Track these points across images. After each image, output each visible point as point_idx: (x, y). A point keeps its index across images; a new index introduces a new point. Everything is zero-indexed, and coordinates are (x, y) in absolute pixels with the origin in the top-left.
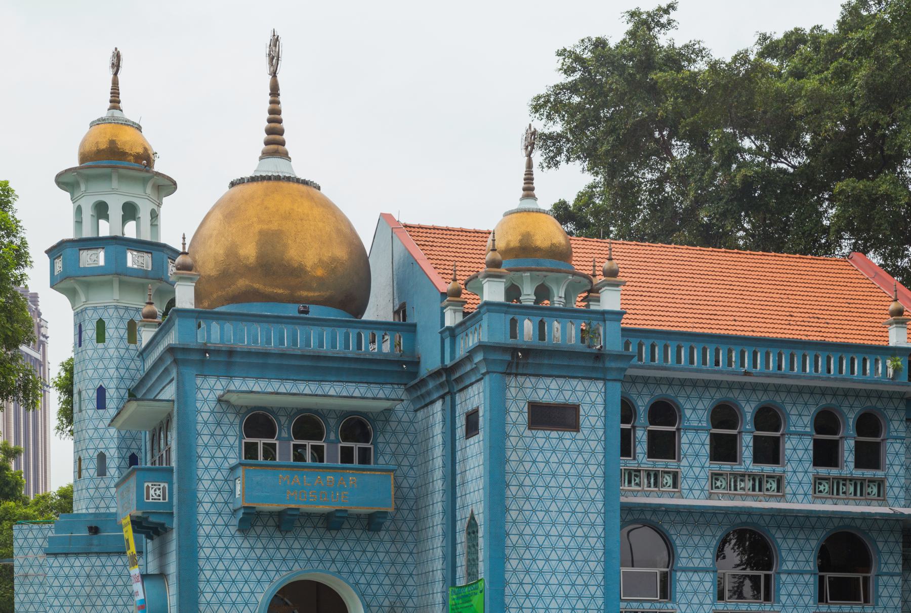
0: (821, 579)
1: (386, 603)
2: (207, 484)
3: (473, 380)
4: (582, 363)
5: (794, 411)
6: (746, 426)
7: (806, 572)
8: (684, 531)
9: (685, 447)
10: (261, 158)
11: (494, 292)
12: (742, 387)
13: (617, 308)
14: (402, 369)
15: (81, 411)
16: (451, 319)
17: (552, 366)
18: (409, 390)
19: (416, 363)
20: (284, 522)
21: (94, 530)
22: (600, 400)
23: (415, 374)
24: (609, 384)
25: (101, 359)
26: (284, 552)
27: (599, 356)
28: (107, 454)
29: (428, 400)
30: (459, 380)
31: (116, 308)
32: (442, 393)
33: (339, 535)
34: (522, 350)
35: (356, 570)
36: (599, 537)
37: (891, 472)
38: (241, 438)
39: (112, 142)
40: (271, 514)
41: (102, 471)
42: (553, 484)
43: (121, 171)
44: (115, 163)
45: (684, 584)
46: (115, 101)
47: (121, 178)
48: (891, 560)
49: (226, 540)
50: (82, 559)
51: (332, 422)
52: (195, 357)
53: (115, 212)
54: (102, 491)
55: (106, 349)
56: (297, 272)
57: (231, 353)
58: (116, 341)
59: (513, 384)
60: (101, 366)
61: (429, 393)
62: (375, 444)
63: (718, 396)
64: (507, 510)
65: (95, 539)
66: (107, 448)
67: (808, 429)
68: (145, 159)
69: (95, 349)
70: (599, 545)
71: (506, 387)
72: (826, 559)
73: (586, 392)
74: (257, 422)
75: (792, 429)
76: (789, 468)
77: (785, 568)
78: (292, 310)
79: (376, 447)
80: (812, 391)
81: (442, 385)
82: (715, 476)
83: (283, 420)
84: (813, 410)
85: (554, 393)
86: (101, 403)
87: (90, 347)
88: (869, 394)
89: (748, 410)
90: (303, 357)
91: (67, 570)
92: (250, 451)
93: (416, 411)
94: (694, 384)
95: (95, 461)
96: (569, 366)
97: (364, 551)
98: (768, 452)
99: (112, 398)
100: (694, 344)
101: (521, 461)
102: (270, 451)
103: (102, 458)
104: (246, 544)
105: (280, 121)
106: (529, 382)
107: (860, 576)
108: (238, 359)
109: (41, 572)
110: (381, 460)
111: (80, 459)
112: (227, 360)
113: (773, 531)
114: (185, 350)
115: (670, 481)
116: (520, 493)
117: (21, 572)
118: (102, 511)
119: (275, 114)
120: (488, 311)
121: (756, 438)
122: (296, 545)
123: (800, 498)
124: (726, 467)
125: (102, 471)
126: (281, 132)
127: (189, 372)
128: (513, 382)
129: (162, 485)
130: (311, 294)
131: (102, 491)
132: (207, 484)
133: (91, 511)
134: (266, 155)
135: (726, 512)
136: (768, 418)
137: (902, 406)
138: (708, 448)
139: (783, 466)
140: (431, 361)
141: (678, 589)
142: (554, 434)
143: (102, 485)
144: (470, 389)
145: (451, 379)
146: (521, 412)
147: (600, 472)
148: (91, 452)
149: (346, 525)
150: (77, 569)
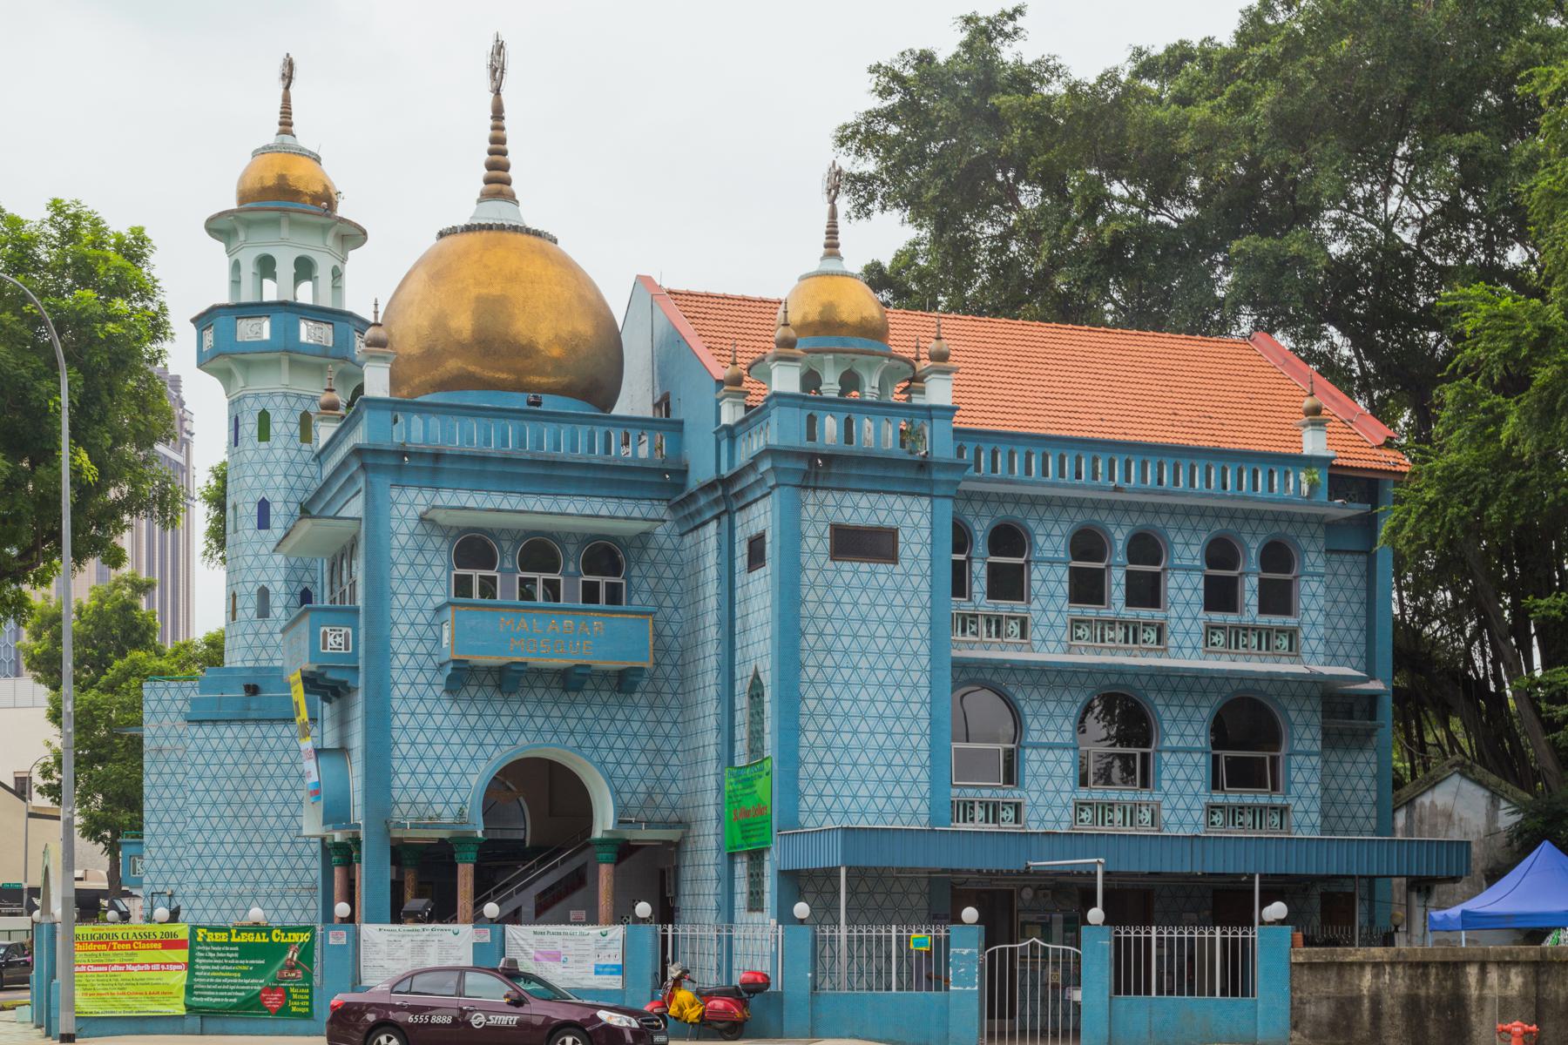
0: (1216, 759)
1: (642, 788)
2: (404, 629)
3: (758, 494)
4: (901, 474)
5: (1179, 539)
6: (1116, 559)
7: (1196, 750)
8: (1035, 695)
9: (1036, 585)
10: (479, 201)
11: (786, 379)
12: (1111, 506)
13: (948, 402)
14: (666, 482)
15: (236, 531)
16: (730, 414)
17: (862, 478)
18: (673, 508)
19: (683, 472)
20: (507, 681)
21: (252, 690)
22: (925, 522)
23: (682, 487)
24: (937, 502)
25: (265, 463)
26: (506, 720)
27: (924, 465)
28: (271, 589)
29: (698, 521)
31: (285, 395)
32: (716, 511)
33: (580, 698)
34: (823, 457)
35: (603, 744)
36: (923, 703)
37: (1307, 619)
38: (450, 569)
39: (282, 177)
40: (489, 670)
41: (264, 611)
42: (863, 632)
43: (293, 215)
44: (285, 204)
45: (1035, 765)
46: (286, 124)
47: (293, 224)
48: (1307, 735)
49: (429, 704)
50: (236, 728)
51: (571, 549)
52: (392, 461)
53: (285, 268)
54: (263, 637)
55: (271, 449)
56: (526, 350)
57: (437, 456)
58: (284, 440)
59: (811, 500)
60: (264, 471)
61: (699, 512)
62: (628, 578)
63: (1080, 518)
64: (802, 666)
65: (254, 702)
66: (270, 581)
67: (1198, 563)
68: (325, 200)
69: (256, 450)
70: (924, 713)
71: (801, 504)
72: (1221, 734)
73: (907, 511)
74: (473, 548)
75: (1177, 562)
76: (1172, 613)
77: (1167, 744)
78: (519, 401)
79: (629, 583)
80: (1202, 512)
81: (716, 502)
82: (1076, 623)
83: (506, 545)
84: (1204, 537)
85: (864, 513)
86: (263, 522)
87: (249, 446)
88: (1277, 517)
89: (1120, 538)
90: (533, 463)
91: (215, 742)
92: (463, 586)
93: (682, 535)
94: (1048, 502)
95: (255, 598)
96: (884, 478)
97: (613, 720)
98: (1145, 591)
99: (277, 514)
100: (1048, 451)
101: (821, 602)
102: (488, 587)
103: (264, 593)
104: (456, 710)
105: (504, 153)
106: (831, 499)
107: (1267, 755)
108: (446, 465)
109: (180, 746)
110: (636, 600)
111: (234, 595)
112: (432, 466)
113: (1152, 696)
114: (377, 452)
115: (1017, 630)
116: (820, 645)
117: (153, 746)
118: (264, 664)
119: (498, 144)
120: (780, 404)
121: (1129, 574)
122: (522, 711)
123: (1187, 652)
124: (1091, 611)
125: (264, 611)
126: (506, 168)
127: (382, 481)
128: (810, 497)
129: (344, 630)
130: (544, 380)
131: (263, 637)
132: (404, 629)
133: (248, 664)
134: (486, 196)
135: (1091, 671)
136: (1145, 547)
137: (1320, 532)
138: (1066, 586)
139: (1165, 610)
140: (702, 470)
141: (1028, 771)
142: (865, 567)
143: (264, 630)
145: (728, 493)
146: (821, 538)
147: (924, 617)
148: (249, 586)
149: (588, 685)
150: (229, 742)
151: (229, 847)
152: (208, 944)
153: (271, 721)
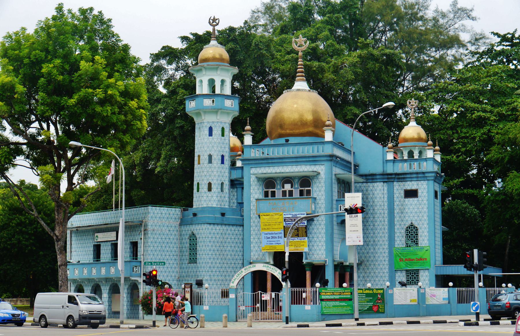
50: (220, 226)
61: (376, 179)
65: (224, 218)
69: (221, 139)
81: (388, 178)
117: (152, 228)
118: (223, 206)
133: (219, 206)
143: (223, 196)
144: (409, 182)
148: (219, 181)
151: (218, 264)
153: (229, 225)
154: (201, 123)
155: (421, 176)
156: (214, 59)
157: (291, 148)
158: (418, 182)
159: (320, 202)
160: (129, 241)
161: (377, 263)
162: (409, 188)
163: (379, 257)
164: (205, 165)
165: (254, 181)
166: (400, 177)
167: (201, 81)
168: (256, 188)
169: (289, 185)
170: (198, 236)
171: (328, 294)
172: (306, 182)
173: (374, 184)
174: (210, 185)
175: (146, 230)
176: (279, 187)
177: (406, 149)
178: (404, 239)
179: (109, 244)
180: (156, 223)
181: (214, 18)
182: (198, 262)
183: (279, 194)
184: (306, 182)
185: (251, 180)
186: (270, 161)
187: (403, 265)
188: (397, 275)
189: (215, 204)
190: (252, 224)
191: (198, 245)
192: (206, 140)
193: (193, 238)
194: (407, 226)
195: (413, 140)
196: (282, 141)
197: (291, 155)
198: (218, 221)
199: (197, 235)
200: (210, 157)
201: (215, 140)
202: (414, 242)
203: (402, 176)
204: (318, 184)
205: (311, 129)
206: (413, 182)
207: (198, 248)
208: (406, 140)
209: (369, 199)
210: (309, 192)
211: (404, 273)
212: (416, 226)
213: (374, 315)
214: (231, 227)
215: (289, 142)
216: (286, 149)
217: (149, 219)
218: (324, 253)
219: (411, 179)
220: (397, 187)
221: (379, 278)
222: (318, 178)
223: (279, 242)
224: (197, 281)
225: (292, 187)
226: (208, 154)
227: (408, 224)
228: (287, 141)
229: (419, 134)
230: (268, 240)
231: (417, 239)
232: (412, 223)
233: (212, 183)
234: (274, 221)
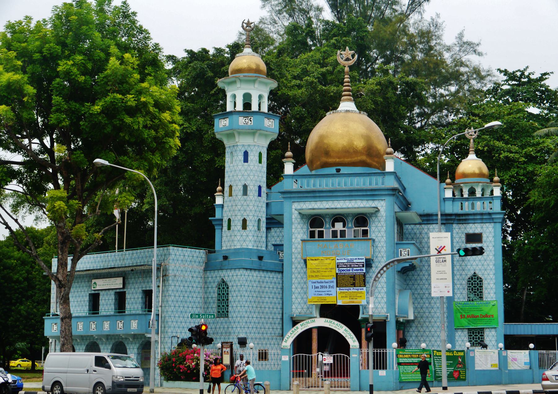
21: (260, 258)
30: (466, 220)
50: (257, 272)
109: (182, 275)
117: (173, 274)
118: (259, 248)
133: (255, 248)
143: (259, 235)
144: (471, 225)
148: (256, 217)
152: (437, 356)
154: (234, 146)
155: (486, 217)
156: (249, 70)
157: (343, 180)
158: (482, 224)
159: (380, 245)
160: (140, 289)
161: (433, 320)
162: (471, 232)
163: (435, 313)
164: (239, 197)
165: (296, 218)
166: (461, 218)
167: (234, 96)
168: (299, 227)
169: (341, 224)
170: (230, 284)
171: (406, 356)
172: (362, 220)
173: (429, 225)
174: (244, 221)
175: (165, 275)
176: (328, 226)
177: (466, 186)
178: (465, 292)
179: (112, 292)
180: (177, 267)
181: (248, 21)
182: (230, 315)
183: (328, 234)
184: (362, 220)
185: (293, 217)
186: (318, 195)
187: (464, 322)
188: (457, 334)
189: (250, 244)
190: (293, 270)
191: (230, 295)
192: (240, 167)
193: (223, 287)
194: (469, 276)
195: (473, 175)
196: (333, 170)
197: (344, 187)
198: (255, 266)
199: (228, 283)
200: (245, 187)
201: (252, 167)
202: (478, 295)
203: (464, 218)
204: (377, 223)
205: (364, 158)
206: (476, 225)
207: (230, 298)
208: (464, 175)
209: (423, 244)
210: (365, 233)
211: (466, 332)
212: (480, 276)
213: (454, 383)
214: (269, 274)
215: (341, 172)
216: (337, 180)
217: (171, 261)
218: (385, 306)
219: (474, 221)
220: (457, 230)
221: (435, 338)
222: (376, 216)
223: (329, 293)
224: (239, 339)
225: (344, 226)
226: (243, 183)
227: (470, 274)
228: (338, 170)
229: (480, 169)
230: (317, 290)
231: (482, 292)
232: (475, 273)
233: (248, 219)
234: (325, 267)
